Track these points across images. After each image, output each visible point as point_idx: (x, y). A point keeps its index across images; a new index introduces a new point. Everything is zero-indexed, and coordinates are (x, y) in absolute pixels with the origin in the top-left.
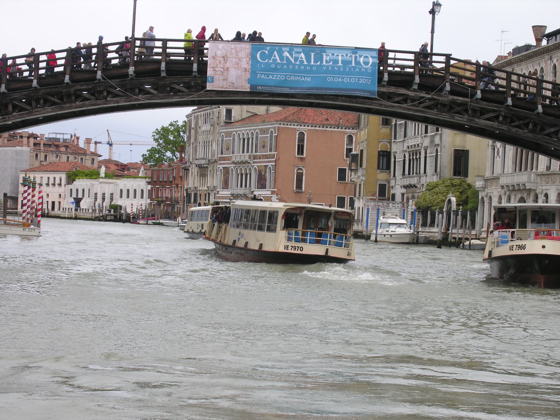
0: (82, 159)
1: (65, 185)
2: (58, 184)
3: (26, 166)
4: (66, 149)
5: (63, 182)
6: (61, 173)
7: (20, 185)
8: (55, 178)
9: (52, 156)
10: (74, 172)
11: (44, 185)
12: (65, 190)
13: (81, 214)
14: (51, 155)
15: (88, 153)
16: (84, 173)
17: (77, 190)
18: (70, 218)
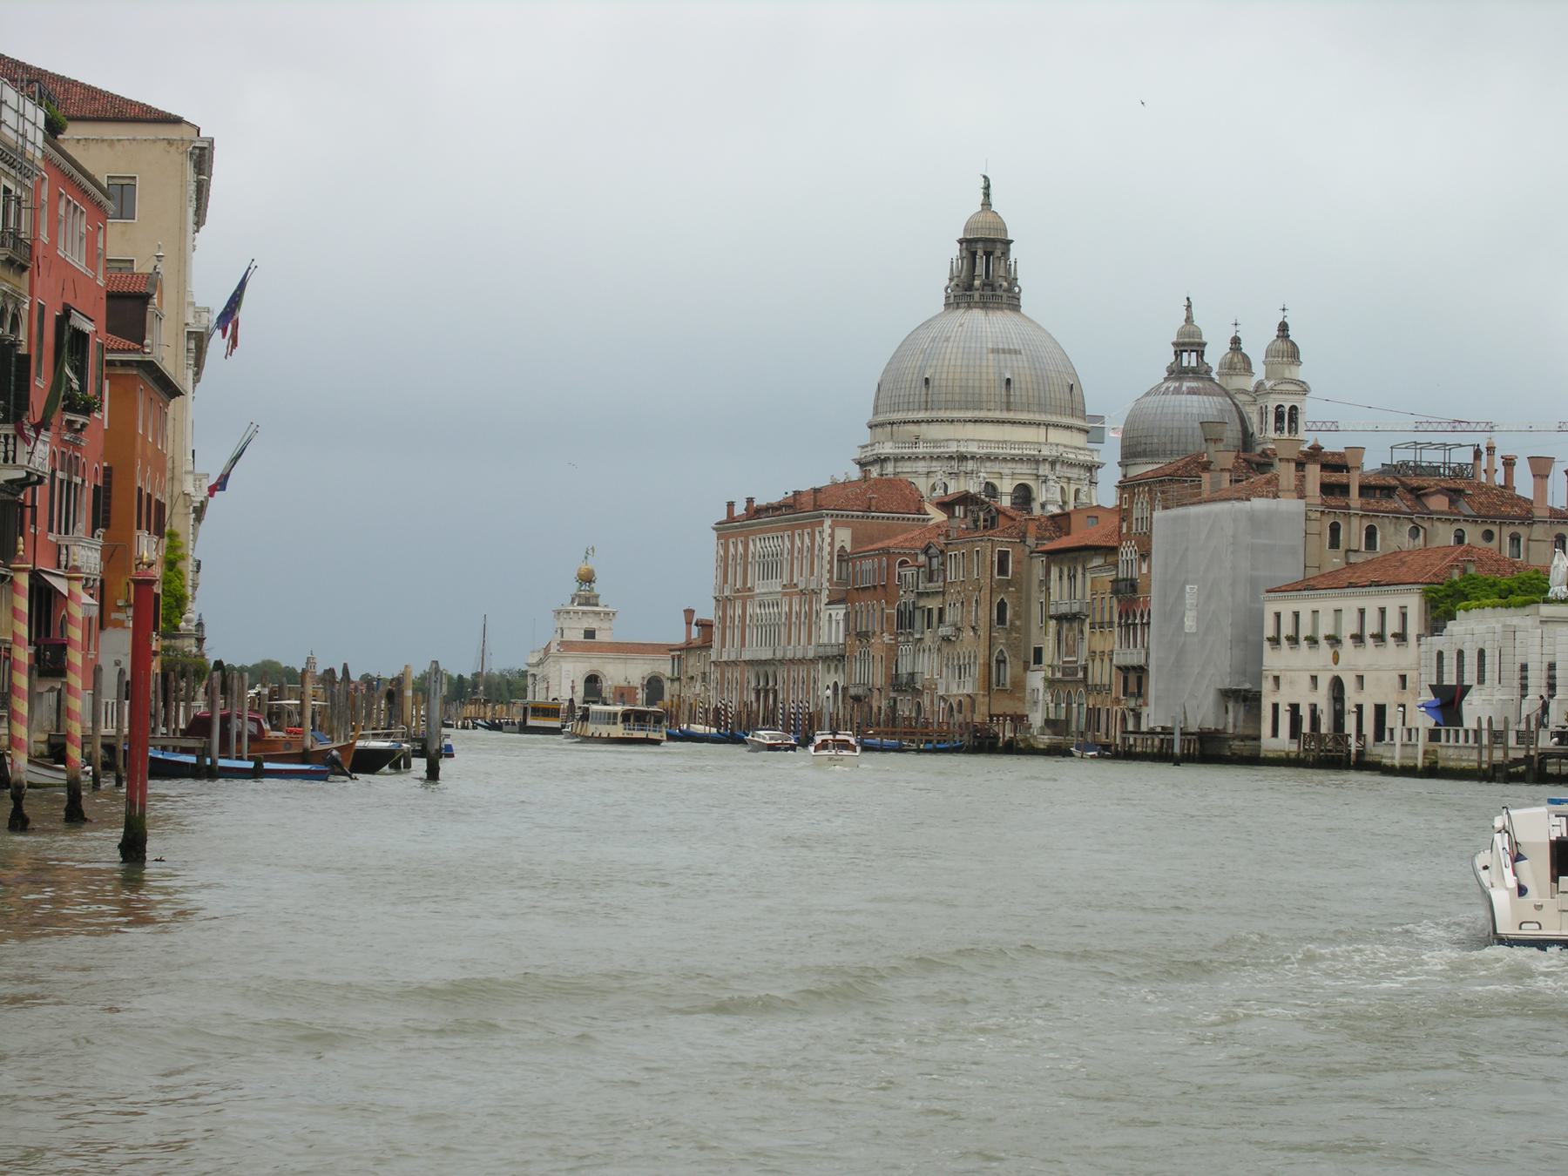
0: (1515, 539)
1: (1419, 637)
2: (1394, 635)
3: (1292, 572)
4: (1452, 502)
5: (1413, 628)
6: (1402, 592)
7: (1266, 644)
8: (1383, 611)
9: (1397, 531)
10: (1452, 585)
11: (1348, 643)
12: (1419, 658)
13: (1451, 752)
14: (1390, 529)
15: (1539, 513)
16: (1494, 585)
17: (1460, 654)
18: (1407, 771)
